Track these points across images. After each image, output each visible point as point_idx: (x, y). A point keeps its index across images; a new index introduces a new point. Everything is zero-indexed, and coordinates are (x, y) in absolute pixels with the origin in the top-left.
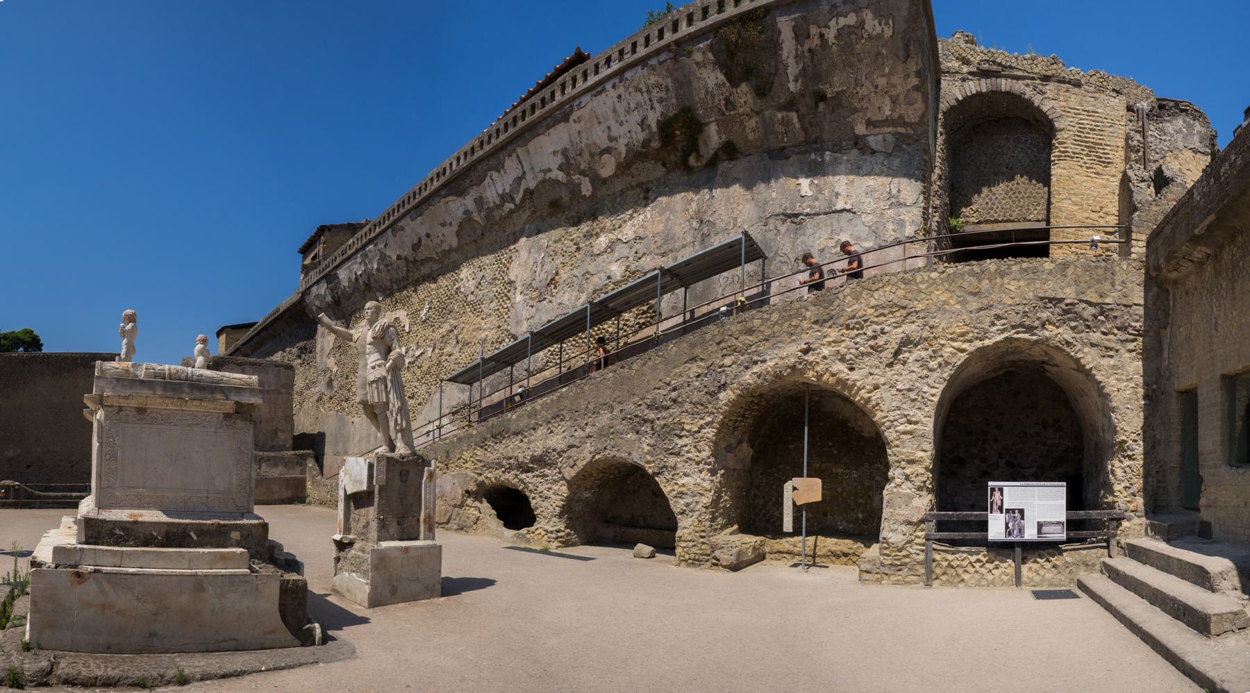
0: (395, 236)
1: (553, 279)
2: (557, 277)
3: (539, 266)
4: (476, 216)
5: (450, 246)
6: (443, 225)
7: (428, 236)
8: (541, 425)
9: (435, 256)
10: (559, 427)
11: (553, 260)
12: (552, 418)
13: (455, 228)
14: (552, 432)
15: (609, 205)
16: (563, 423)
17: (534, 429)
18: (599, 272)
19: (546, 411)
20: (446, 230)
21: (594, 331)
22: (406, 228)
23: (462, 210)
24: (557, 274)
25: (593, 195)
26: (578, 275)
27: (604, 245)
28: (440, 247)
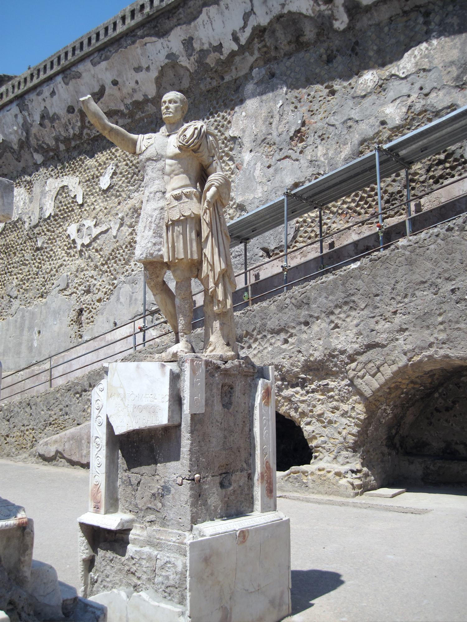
0: (67, 84)
1: (298, 131)
2: (303, 129)
3: (277, 117)
4: (184, 61)
5: (145, 95)
6: (138, 69)
7: (115, 83)
8: (317, 318)
9: (122, 108)
10: (348, 320)
11: (296, 108)
12: (336, 306)
13: (154, 74)
14: (337, 326)
15: (374, 37)
16: (353, 313)
17: (306, 324)
18: (368, 117)
19: (326, 298)
20: (140, 76)
21: (365, 192)
22: (84, 75)
23: (164, 53)
24: (303, 124)
25: (349, 28)
26: (336, 123)
27: (371, 84)
28: (131, 96)
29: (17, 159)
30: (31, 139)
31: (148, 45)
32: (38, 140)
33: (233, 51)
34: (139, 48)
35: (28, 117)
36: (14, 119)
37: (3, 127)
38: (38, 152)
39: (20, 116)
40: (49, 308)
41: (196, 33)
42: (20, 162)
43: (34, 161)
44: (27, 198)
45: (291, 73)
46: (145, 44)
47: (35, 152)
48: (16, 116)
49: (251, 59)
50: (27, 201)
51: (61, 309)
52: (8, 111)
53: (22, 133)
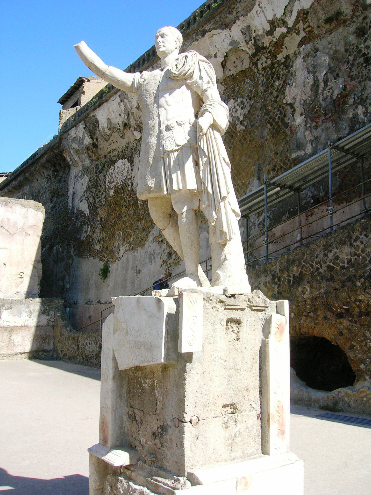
3: (322, 85)
29: (121, 137)
30: (131, 120)
31: (214, 36)
32: (136, 121)
33: (283, 33)
34: (208, 40)
35: (128, 104)
36: (118, 106)
37: (111, 113)
38: (137, 131)
39: (122, 104)
40: (146, 252)
41: (252, 22)
42: (124, 139)
43: (134, 138)
44: (129, 166)
45: (332, 46)
46: (212, 36)
47: (134, 130)
48: (119, 104)
49: (299, 38)
50: (130, 169)
51: (155, 253)
52: (113, 100)
53: (124, 116)
